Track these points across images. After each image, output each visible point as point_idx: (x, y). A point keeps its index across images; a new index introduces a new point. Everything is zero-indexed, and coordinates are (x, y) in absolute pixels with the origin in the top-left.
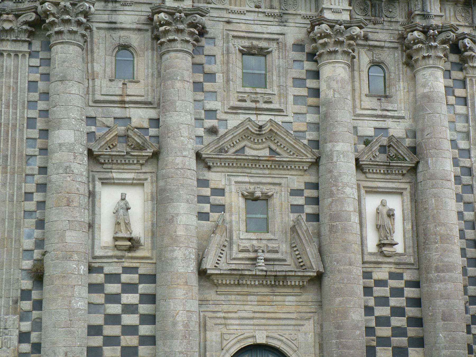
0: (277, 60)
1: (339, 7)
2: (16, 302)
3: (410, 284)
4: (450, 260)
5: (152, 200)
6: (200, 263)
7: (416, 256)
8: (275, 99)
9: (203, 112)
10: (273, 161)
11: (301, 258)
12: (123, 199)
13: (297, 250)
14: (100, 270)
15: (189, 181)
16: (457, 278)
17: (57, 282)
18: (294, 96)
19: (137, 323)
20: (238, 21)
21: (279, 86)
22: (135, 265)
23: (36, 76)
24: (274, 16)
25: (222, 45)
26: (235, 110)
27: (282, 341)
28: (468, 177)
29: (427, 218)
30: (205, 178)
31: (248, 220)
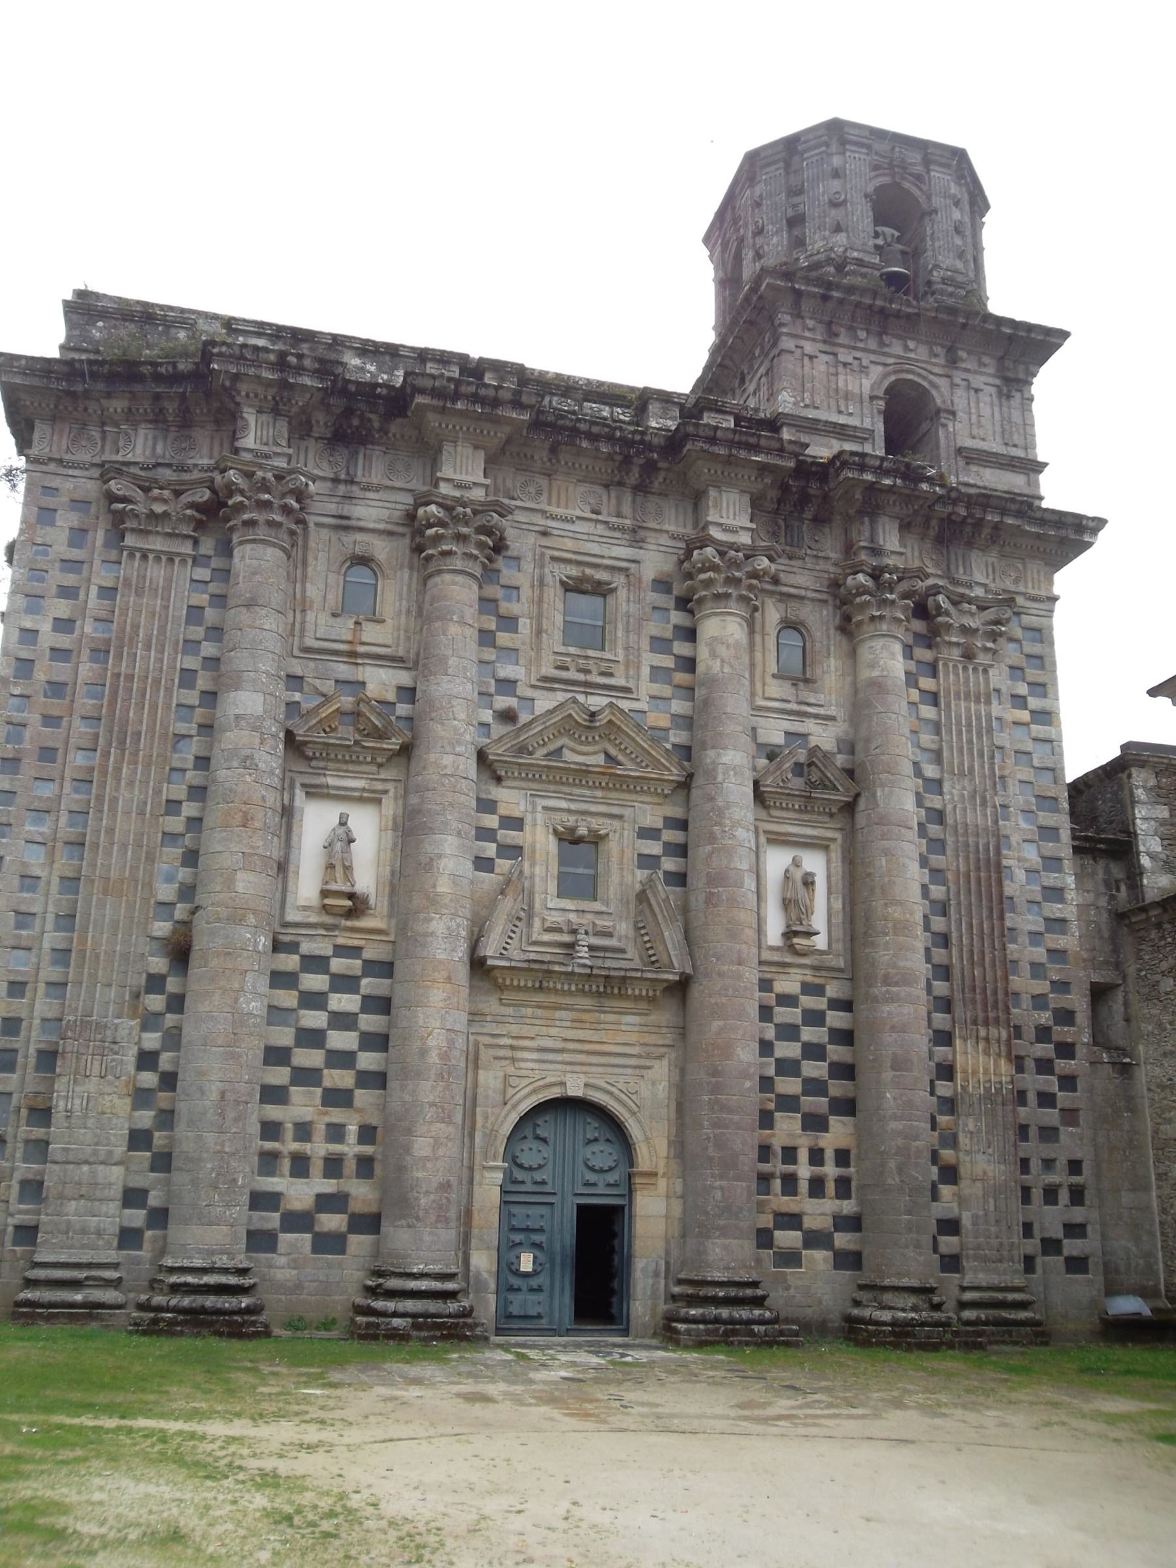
0: (624, 604)
1: (734, 523)
2: (136, 996)
3: (835, 1004)
4: (909, 964)
5: (395, 829)
6: (474, 947)
7: (849, 957)
8: (619, 670)
9: (493, 681)
10: (611, 775)
11: (652, 948)
12: (343, 823)
13: (647, 934)
14: (293, 947)
15: (463, 798)
16: (918, 997)
17: (214, 963)
18: (652, 667)
19: (355, 1046)
20: (562, 533)
21: (627, 649)
22: (356, 943)
23: (202, 599)
24: (622, 529)
25: (531, 570)
26: (548, 683)
27: (611, 1094)
28: (937, 827)
29: (872, 890)
30: (490, 797)
31: (562, 878)
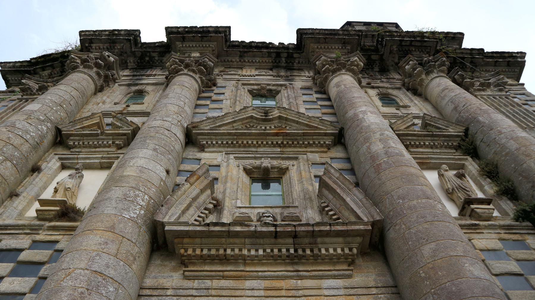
13: (331, 210)
22: (53, 238)
